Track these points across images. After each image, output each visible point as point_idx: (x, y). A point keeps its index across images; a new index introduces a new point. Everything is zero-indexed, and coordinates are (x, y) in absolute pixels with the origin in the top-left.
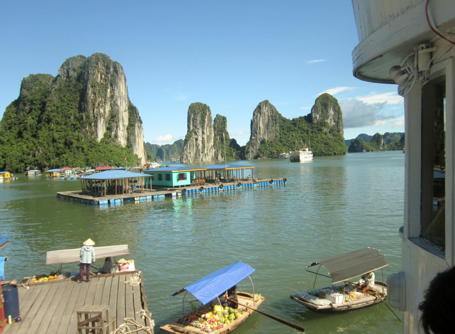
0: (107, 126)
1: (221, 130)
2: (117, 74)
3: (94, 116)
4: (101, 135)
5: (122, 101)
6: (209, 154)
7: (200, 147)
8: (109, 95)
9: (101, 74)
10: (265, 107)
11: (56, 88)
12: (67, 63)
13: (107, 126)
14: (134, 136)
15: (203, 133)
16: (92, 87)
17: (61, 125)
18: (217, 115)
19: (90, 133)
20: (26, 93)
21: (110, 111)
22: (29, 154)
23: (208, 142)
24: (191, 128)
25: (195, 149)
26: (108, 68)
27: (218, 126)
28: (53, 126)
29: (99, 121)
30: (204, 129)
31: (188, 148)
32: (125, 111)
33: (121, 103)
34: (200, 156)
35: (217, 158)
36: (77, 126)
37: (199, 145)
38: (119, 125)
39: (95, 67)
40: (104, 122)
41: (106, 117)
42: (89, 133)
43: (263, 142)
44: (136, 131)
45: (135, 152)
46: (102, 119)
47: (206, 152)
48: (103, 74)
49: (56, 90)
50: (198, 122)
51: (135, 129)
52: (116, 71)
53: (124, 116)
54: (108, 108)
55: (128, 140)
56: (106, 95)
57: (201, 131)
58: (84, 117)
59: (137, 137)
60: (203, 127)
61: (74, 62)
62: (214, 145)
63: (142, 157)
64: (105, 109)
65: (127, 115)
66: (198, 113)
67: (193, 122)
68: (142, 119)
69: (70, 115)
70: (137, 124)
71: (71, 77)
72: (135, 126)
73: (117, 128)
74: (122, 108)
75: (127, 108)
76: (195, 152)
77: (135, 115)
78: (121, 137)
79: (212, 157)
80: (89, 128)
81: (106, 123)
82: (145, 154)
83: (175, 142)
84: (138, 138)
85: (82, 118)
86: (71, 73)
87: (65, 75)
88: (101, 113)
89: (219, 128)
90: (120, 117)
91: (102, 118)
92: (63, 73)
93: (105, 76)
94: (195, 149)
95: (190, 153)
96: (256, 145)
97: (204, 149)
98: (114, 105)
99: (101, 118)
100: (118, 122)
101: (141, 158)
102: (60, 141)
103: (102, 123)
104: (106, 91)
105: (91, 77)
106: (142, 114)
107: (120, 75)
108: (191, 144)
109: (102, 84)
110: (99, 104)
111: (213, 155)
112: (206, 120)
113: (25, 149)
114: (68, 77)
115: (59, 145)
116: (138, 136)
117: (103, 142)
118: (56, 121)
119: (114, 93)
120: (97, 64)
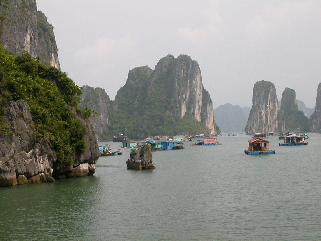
6: (272, 125)
7: (264, 120)
15: (266, 107)
18: (285, 88)
23: (271, 115)
25: (258, 121)
32: (200, 95)
37: (262, 118)
38: (196, 106)
47: (269, 124)
54: (188, 94)
70: (208, 104)
75: (201, 93)
94: (258, 121)
95: (253, 125)
111: (277, 126)
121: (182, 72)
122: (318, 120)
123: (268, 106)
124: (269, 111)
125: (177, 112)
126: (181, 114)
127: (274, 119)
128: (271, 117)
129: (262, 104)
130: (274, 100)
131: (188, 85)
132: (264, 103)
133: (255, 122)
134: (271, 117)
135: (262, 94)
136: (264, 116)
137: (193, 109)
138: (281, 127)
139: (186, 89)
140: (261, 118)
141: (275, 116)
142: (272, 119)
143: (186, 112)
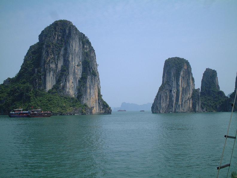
4: (49, 86)
5: (74, 57)
9: (58, 36)
15: (178, 85)
18: (207, 69)
21: (62, 66)
23: (183, 94)
29: (48, 74)
32: (77, 66)
37: (173, 96)
41: (57, 71)
46: (52, 73)
47: (180, 103)
51: (86, 81)
54: (60, 64)
62: (192, 97)
64: (57, 65)
74: (74, 63)
75: (81, 63)
88: (52, 67)
90: (71, 70)
94: (168, 100)
99: (50, 72)
100: (68, 75)
111: (191, 106)
112: (182, 73)
121: (56, 38)
124: (181, 89)
125: (40, 85)
126: (45, 88)
129: (173, 82)
131: (62, 53)
132: (174, 80)
136: (175, 95)
137: (65, 82)
139: (58, 57)
141: (189, 96)
142: (184, 99)
143: (54, 84)
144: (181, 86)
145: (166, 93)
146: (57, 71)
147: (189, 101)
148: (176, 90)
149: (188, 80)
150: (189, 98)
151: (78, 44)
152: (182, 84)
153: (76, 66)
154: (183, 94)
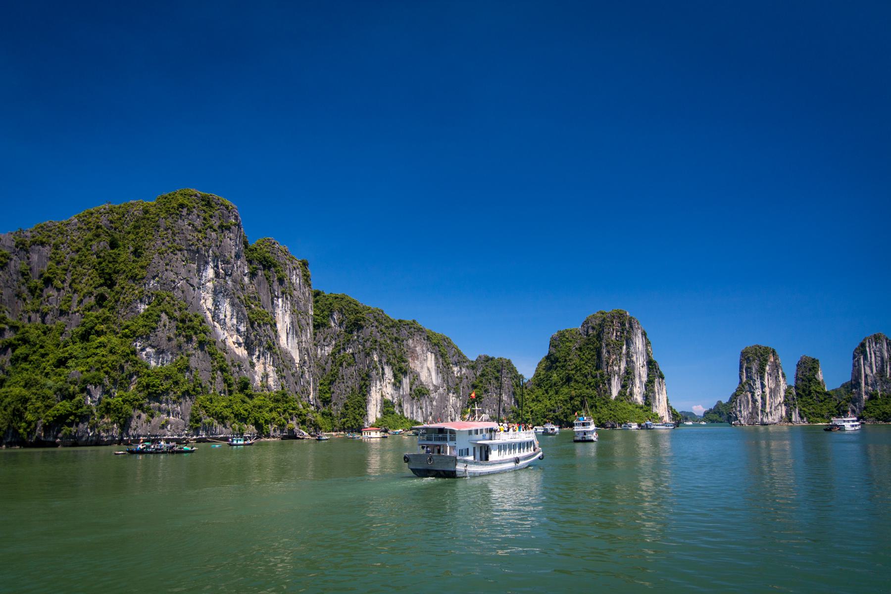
0: (622, 382)
1: (807, 378)
2: (633, 330)
3: (608, 374)
4: (615, 392)
5: (638, 357)
6: (774, 412)
8: (624, 351)
10: (874, 345)
11: (576, 346)
12: (586, 323)
13: (622, 382)
14: (654, 392)
15: (763, 386)
16: (607, 345)
17: (579, 383)
19: (604, 391)
20: (553, 351)
21: (625, 368)
22: (551, 410)
23: (771, 396)
24: (744, 379)
25: (750, 406)
26: (623, 324)
27: (803, 372)
28: (572, 384)
30: (764, 380)
31: (738, 404)
33: (637, 358)
34: (758, 415)
35: (790, 420)
36: (592, 384)
37: (756, 401)
39: (610, 325)
40: (618, 379)
41: (621, 374)
42: (602, 391)
43: (872, 397)
44: (656, 388)
45: (655, 410)
46: (616, 377)
47: (768, 410)
48: (618, 331)
49: (576, 349)
50: (754, 371)
51: (654, 384)
52: (631, 327)
53: (642, 372)
54: (623, 365)
55: (646, 397)
56: (621, 353)
57: (759, 383)
58: (598, 375)
59: (657, 394)
60: (762, 378)
61: (593, 320)
63: (664, 415)
64: (619, 367)
65: (646, 370)
66: (754, 360)
67: (747, 372)
68: (663, 373)
69: (587, 373)
70: (656, 380)
71: (590, 335)
72: (654, 383)
73: (632, 385)
74: (638, 364)
75: (645, 363)
76: (750, 410)
77: (655, 370)
78: (638, 394)
79: (782, 417)
80: (603, 386)
81: (621, 380)
82: (669, 412)
83: (843, 386)
84: (659, 395)
85: (596, 376)
86: (591, 332)
87: (585, 333)
89: (805, 376)
90: (637, 373)
91: (616, 375)
92: (583, 332)
93: (621, 332)
94: (750, 406)
95: (740, 411)
96: (859, 401)
97: (765, 407)
98: (630, 362)
99: (615, 375)
101: (663, 417)
102: (576, 398)
103: (616, 380)
104: (621, 348)
105: (605, 336)
106: (663, 369)
107: (635, 330)
108: (743, 399)
109: (617, 340)
110: (613, 362)
111: (784, 414)
112: (767, 368)
113: (549, 405)
114: (587, 335)
115: (576, 403)
116: (658, 392)
117: (617, 399)
118: (575, 379)
119: (630, 349)
120: (612, 322)
122: (857, 405)
123: (766, 383)
124: (767, 390)
125: (605, 392)
127: (778, 403)
128: (771, 400)
130: (776, 374)
132: (757, 378)
133: (743, 408)
134: (771, 400)
135: (755, 366)
136: (759, 399)
138: (791, 415)
140: (755, 401)
142: (773, 404)
144: (767, 387)
145: (747, 397)
146: (621, 374)
147: (780, 407)
148: (761, 392)
149: (776, 378)
150: (780, 403)
151: (641, 340)
152: (768, 383)
153: (641, 368)
154: (772, 398)
